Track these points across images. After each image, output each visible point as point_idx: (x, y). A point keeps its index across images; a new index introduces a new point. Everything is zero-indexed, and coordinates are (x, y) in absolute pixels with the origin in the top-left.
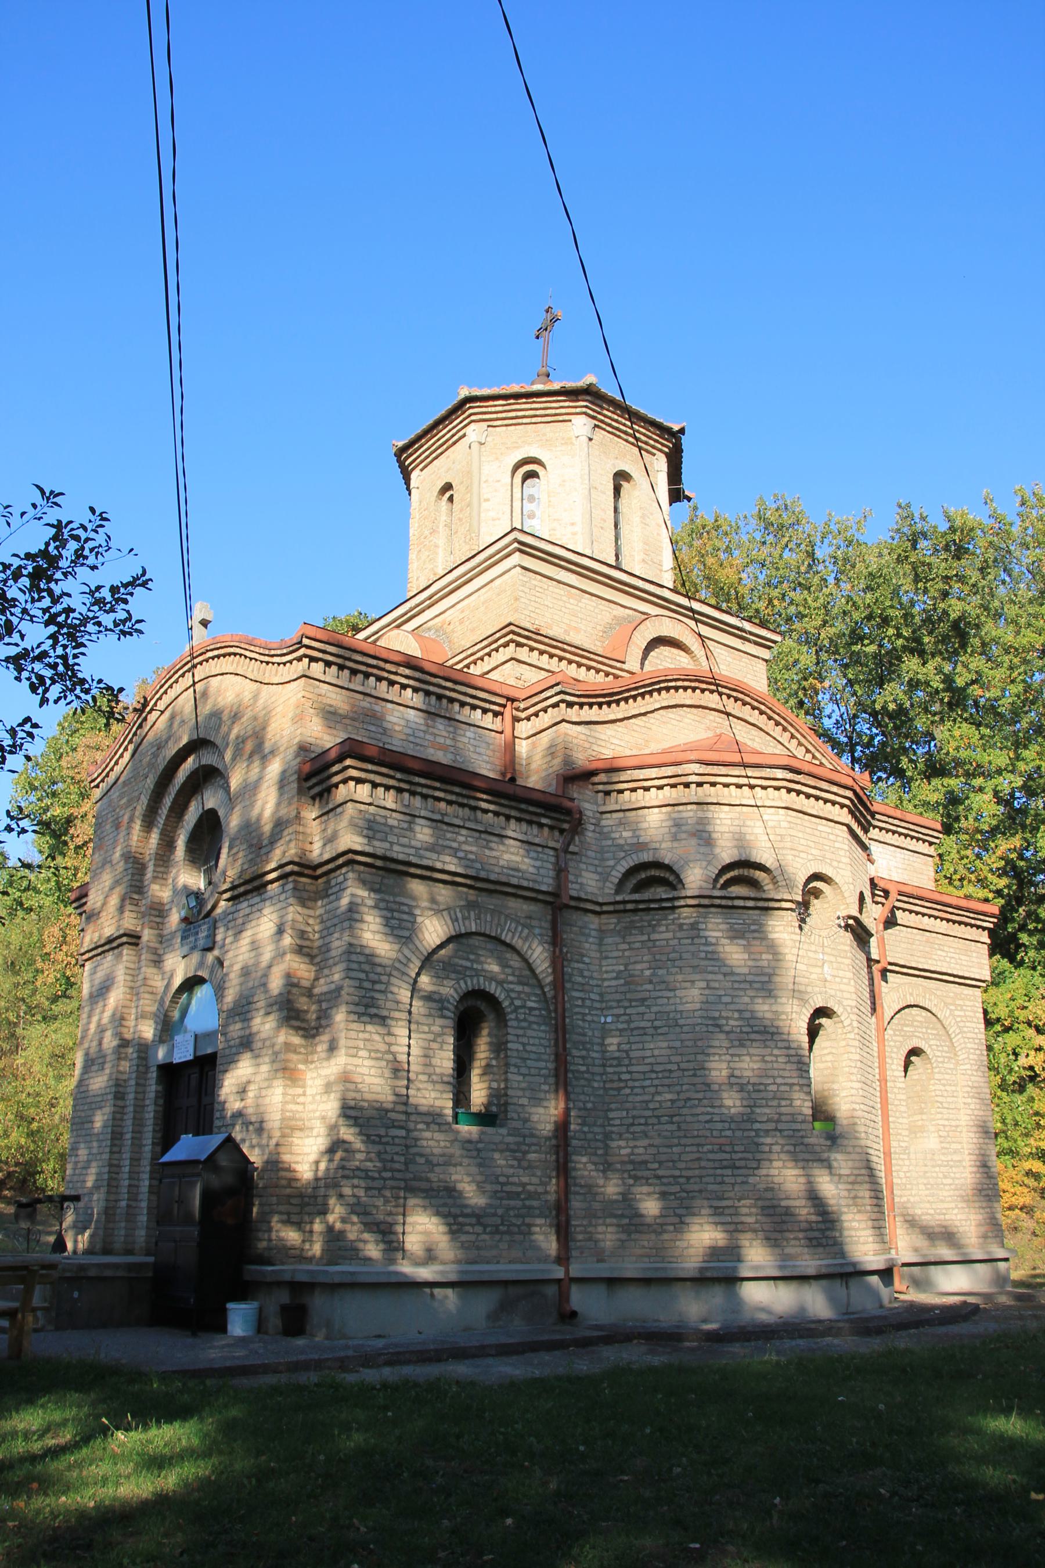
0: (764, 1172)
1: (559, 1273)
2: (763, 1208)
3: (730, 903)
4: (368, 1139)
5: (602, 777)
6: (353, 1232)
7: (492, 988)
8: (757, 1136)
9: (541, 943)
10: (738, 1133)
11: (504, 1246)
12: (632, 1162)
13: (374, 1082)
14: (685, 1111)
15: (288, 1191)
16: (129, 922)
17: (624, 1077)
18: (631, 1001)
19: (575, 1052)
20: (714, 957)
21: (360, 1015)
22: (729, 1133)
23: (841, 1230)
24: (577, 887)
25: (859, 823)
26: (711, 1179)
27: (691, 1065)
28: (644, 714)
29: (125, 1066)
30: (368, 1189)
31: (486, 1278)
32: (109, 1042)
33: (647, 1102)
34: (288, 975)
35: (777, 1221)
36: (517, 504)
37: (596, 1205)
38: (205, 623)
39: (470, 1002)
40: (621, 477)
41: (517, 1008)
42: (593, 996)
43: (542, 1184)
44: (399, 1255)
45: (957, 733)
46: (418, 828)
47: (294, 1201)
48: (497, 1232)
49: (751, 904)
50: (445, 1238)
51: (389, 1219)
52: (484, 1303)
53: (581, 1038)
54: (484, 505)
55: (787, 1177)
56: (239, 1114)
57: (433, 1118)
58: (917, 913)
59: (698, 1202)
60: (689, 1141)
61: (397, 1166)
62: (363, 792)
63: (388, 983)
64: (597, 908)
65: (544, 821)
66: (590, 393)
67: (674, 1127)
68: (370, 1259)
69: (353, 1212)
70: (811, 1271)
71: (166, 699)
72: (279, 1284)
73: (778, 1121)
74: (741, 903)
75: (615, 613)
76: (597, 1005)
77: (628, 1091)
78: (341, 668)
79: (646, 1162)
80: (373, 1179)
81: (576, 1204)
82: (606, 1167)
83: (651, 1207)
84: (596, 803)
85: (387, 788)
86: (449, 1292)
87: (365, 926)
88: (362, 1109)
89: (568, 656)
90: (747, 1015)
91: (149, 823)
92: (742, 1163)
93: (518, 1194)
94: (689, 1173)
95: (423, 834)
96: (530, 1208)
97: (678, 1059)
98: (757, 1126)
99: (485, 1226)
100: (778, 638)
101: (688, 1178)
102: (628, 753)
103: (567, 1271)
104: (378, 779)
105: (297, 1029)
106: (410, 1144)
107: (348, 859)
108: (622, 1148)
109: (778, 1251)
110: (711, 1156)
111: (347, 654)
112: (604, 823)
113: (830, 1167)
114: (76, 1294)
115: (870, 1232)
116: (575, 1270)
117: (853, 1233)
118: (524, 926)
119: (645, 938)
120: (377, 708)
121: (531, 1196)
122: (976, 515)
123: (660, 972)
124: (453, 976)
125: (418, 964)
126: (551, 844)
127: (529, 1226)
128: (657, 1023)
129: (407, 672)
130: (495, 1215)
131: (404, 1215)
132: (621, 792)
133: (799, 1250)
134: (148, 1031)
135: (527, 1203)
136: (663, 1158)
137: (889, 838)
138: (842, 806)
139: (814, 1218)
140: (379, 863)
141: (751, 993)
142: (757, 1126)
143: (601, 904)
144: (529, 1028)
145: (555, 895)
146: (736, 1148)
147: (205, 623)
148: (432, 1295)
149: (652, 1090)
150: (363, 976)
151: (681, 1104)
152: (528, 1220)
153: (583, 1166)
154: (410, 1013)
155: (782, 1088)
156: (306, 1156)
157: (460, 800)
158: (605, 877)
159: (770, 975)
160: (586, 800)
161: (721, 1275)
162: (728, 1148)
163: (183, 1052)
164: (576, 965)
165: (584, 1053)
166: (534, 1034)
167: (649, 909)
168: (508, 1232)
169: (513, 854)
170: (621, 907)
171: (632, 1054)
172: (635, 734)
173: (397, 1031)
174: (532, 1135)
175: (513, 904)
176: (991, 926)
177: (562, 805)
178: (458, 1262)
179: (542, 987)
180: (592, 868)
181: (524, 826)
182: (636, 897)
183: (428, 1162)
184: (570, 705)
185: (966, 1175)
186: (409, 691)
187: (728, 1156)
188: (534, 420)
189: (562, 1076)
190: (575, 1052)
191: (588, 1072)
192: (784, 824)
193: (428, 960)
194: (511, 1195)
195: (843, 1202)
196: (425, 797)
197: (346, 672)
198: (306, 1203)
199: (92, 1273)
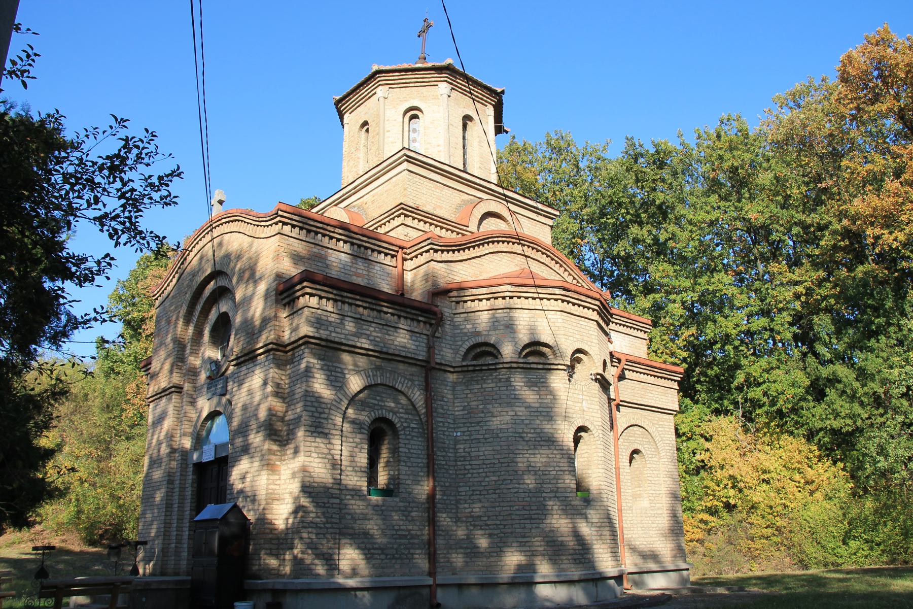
0: (549, 521)
1: (430, 581)
2: (548, 542)
3: (528, 366)
4: (317, 505)
5: (455, 293)
6: (308, 559)
7: (390, 416)
9: (419, 390)
10: (534, 499)
11: (397, 566)
12: (472, 517)
13: (320, 471)
14: (503, 487)
15: (270, 536)
16: (176, 379)
17: (468, 467)
18: (471, 423)
21: (312, 432)
22: (528, 499)
23: (593, 554)
25: (604, 320)
26: (518, 526)
27: (506, 460)
29: (174, 464)
30: (317, 534)
32: (164, 450)
33: (481, 482)
34: (270, 409)
35: (555, 549)
36: (406, 134)
37: (452, 542)
38: (221, 202)
40: (467, 119)
41: (405, 428)
42: (449, 421)
43: (420, 530)
44: (336, 572)
45: (661, 268)
46: (346, 323)
47: (273, 542)
48: (394, 558)
49: (540, 366)
50: (363, 562)
51: (330, 551)
54: (387, 134)
55: (560, 523)
56: (241, 491)
57: (356, 493)
58: (637, 372)
59: (510, 540)
60: (505, 504)
61: (334, 520)
62: (314, 301)
63: (329, 414)
64: (452, 370)
65: (420, 318)
66: (448, 69)
67: (497, 496)
68: (319, 575)
69: (309, 548)
70: (576, 578)
71: (198, 247)
72: (265, 591)
74: (535, 366)
77: (470, 475)
78: (301, 228)
79: (481, 516)
80: (321, 528)
81: (440, 542)
82: (457, 520)
83: (483, 543)
84: (451, 308)
85: (328, 299)
86: (366, 593)
87: (315, 380)
88: (314, 487)
90: (538, 431)
91: (187, 322)
92: (536, 516)
93: (406, 536)
94: (505, 523)
95: (350, 326)
96: (414, 543)
97: (499, 456)
98: (544, 495)
99: (387, 555)
100: (558, 213)
101: (505, 525)
102: (470, 279)
103: (435, 580)
104: (323, 294)
105: (275, 441)
106: (342, 507)
107: (305, 341)
108: (465, 509)
109: (556, 566)
110: (518, 513)
111: (305, 220)
112: (455, 320)
113: (586, 518)
114: (144, 599)
115: (609, 555)
116: (440, 579)
118: (409, 380)
119: (479, 386)
120: (323, 252)
121: (413, 537)
122: (673, 144)
123: (488, 406)
124: (367, 409)
125: (347, 402)
126: (425, 332)
127: (413, 554)
128: (486, 436)
129: (340, 231)
130: (392, 548)
131: (339, 549)
132: (466, 302)
133: (568, 566)
134: (187, 443)
135: (411, 541)
136: (491, 514)
137: (621, 329)
138: (594, 310)
139: (577, 547)
140: (323, 343)
141: (542, 418)
142: (544, 495)
144: (412, 439)
145: (427, 362)
147: (221, 202)
148: (356, 595)
149: (484, 475)
150: (314, 409)
151: (500, 482)
152: (412, 551)
153: (444, 519)
154: (342, 431)
155: (559, 473)
156: (281, 515)
157: (371, 306)
158: (456, 352)
159: (551, 408)
160: (445, 307)
161: (524, 580)
162: (527, 508)
163: (208, 455)
164: (439, 403)
167: (482, 370)
169: (402, 339)
170: (465, 369)
171: (473, 454)
173: (334, 441)
174: (414, 502)
175: (401, 366)
177: (431, 309)
178: (371, 576)
179: (419, 416)
180: (448, 346)
181: (409, 321)
182: (474, 363)
183: (352, 518)
184: (436, 251)
185: (664, 521)
186: (342, 242)
187: (527, 512)
189: (431, 468)
190: (439, 453)
191: (446, 464)
192: (560, 321)
193: (352, 400)
195: (594, 538)
196: (350, 304)
197: (304, 231)
198: (280, 542)
199: (154, 586)
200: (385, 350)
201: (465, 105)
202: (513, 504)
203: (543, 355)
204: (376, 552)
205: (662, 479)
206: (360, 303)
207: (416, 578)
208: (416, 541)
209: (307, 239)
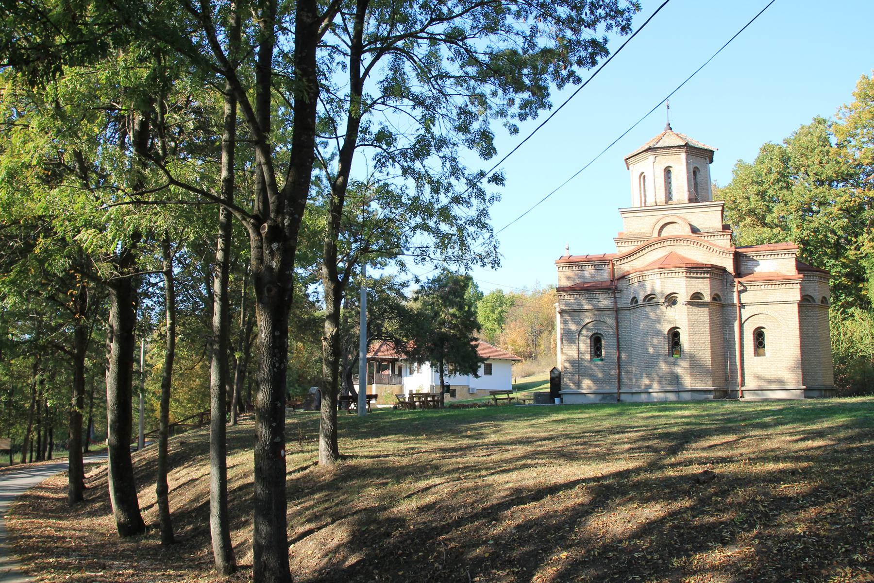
20: (648, 317)
52: (599, 397)
66: (649, 149)
160: (622, 284)
169: (605, 302)
201: (664, 161)
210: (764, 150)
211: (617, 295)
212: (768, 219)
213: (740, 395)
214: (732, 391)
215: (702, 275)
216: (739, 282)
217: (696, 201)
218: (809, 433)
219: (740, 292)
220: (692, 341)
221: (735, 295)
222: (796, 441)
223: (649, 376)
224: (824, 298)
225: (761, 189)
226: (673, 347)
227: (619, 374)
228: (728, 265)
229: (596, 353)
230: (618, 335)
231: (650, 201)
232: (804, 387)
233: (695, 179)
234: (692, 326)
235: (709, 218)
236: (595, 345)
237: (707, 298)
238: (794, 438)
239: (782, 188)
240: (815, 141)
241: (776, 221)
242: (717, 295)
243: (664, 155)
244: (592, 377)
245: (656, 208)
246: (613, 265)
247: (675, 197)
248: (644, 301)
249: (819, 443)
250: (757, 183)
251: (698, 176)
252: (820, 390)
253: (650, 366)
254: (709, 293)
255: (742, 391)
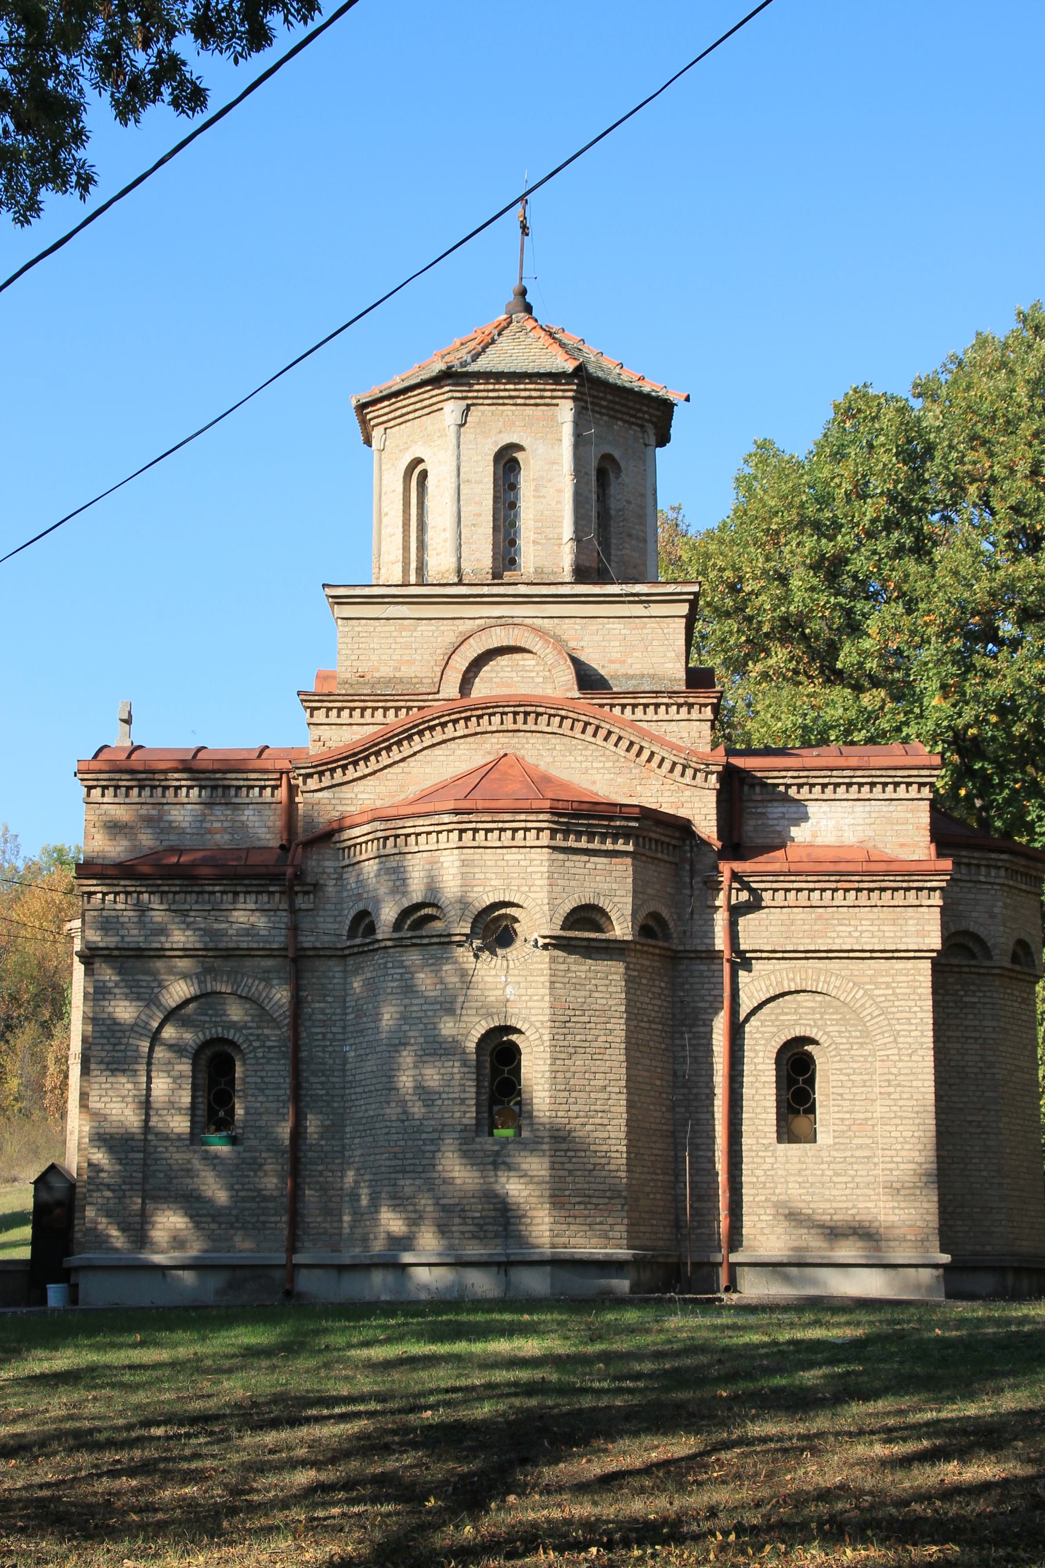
1: (281, 1258)
7: (231, 1035)
8: (425, 1144)
10: (410, 1143)
19: (313, 1079)
21: (113, 1071)
22: (402, 1143)
24: (312, 939)
26: (386, 1182)
28: (403, 760)
31: (217, 1262)
35: (450, 1216)
39: (208, 1052)
42: (334, 1030)
48: (232, 1227)
52: (215, 1281)
53: (321, 1067)
54: (385, 520)
64: (339, 953)
65: (271, 889)
66: (447, 377)
73: (442, 1131)
75: (461, 628)
76: (340, 1037)
89: (369, 704)
92: (411, 1168)
93: (254, 1198)
98: (424, 1136)
112: (345, 876)
116: (299, 1258)
117: (523, 1228)
118: (261, 980)
121: (265, 1199)
127: (264, 1223)
130: (230, 1214)
135: (262, 1205)
142: (424, 1136)
143: (343, 949)
144: (268, 1063)
145: (285, 949)
146: (408, 1156)
150: (105, 1041)
157: (184, 889)
162: (400, 1156)
164: (317, 1005)
165: (323, 1079)
166: (272, 1068)
168: (243, 1228)
172: (390, 783)
175: (248, 963)
176: (944, 884)
181: (253, 897)
187: (400, 1162)
188: (417, 414)
190: (313, 1079)
191: (327, 1094)
194: (244, 1199)
200: (211, 945)
202: (382, 1150)
203: (432, 918)
204: (203, 1219)
205: (877, 1090)
206: (166, 889)
207: (267, 1254)
208: (270, 1205)
209: (117, 800)
210: (848, 412)
211: (301, 902)
212: (846, 658)
213: (723, 1282)
214: (698, 1266)
215: (609, 846)
216: (735, 876)
217: (601, 576)
218: (951, 1433)
219: (736, 912)
220: (562, 1081)
221: (721, 919)
222: (905, 1462)
223: (399, 1202)
224: (1022, 944)
225: (828, 547)
226: (493, 1101)
227: (296, 1196)
228: (701, 810)
229: (211, 1113)
230: (297, 1048)
231: (440, 562)
232: (946, 1258)
233: (603, 496)
234: (563, 1023)
235: (642, 641)
236: (212, 1082)
237: (621, 929)
238: (898, 1449)
239: (899, 551)
240: (1022, 394)
241: (872, 665)
242: (655, 916)
243: (498, 401)
244: (193, 1204)
245: (458, 593)
246: (292, 790)
247: (530, 557)
248: (398, 925)
249: (984, 1470)
250: (817, 526)
251: (613, 489)
252: (1000, 1270)
253: (406, 1167)
254: (628, 910)
255: (733, 1267)
